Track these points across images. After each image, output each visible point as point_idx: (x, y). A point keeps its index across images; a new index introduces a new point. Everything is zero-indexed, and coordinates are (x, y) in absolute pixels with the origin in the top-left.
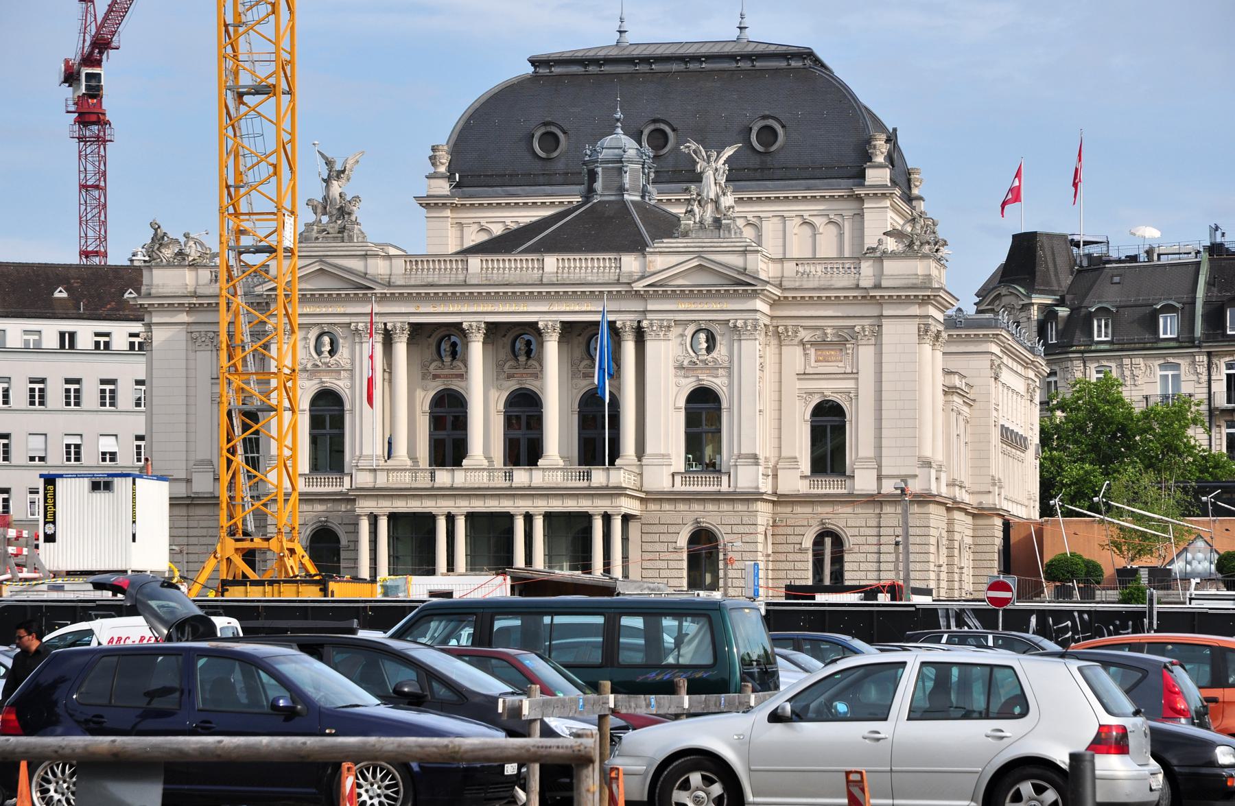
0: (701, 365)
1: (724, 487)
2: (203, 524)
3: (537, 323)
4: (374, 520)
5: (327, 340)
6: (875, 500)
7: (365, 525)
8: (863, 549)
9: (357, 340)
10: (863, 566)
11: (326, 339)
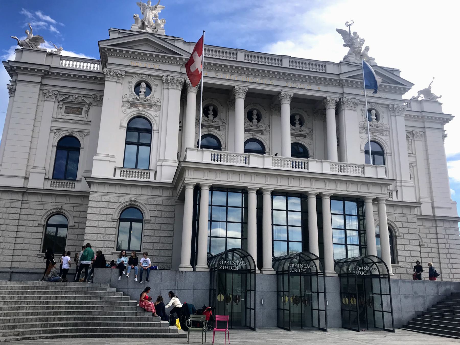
0: (375, 127)
1: (395, 199)
2: (32, 206)
3: (280, 92)
4: (198, 189)
5: (143, 86)
6: (434, 219)
7: (190, 193)
8: (429, 245)
9: (166, 86)
10: (431, 255)
11: (143, 85)
